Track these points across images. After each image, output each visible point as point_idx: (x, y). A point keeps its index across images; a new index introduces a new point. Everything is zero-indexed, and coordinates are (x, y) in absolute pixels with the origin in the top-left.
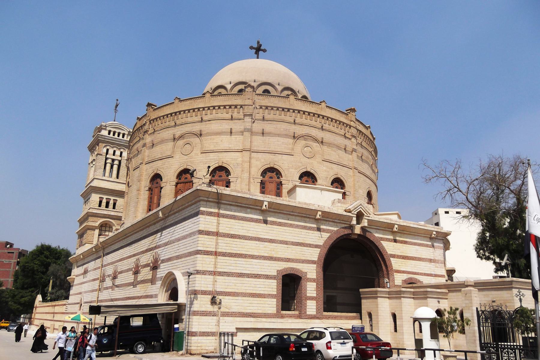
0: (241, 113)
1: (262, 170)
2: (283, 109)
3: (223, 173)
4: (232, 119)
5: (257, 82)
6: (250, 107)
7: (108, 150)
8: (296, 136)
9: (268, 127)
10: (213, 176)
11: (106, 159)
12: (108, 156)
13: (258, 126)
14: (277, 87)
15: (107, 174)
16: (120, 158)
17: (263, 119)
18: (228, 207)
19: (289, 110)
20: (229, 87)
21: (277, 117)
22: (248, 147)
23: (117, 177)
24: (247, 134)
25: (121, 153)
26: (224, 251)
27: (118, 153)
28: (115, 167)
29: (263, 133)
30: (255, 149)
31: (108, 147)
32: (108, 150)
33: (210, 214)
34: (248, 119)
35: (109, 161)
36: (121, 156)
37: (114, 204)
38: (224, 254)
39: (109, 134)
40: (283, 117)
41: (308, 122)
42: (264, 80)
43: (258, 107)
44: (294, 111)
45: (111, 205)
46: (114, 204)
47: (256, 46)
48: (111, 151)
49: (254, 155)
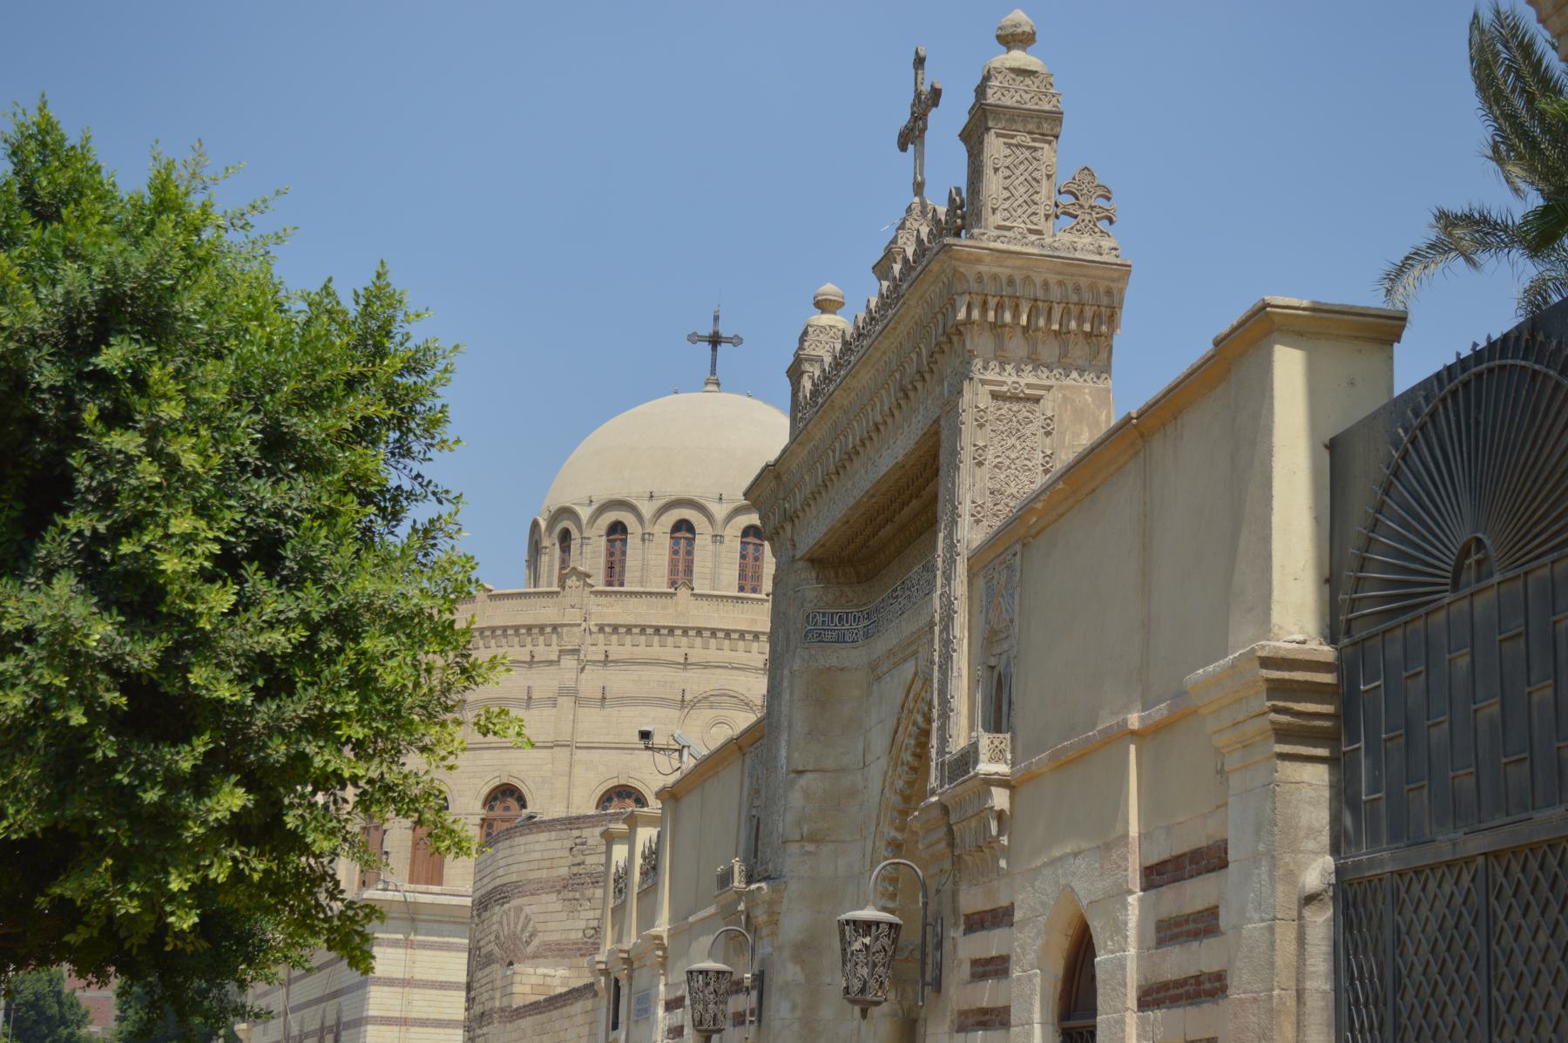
0: (555, 648)
1: (599, 793)
2: (657, 630)
3: (512, 802)
4: (531, 663)
5: (659, 498)
6: (576, 629)
8: (688, 697)
9: (620, 681)
10: (491, 808)
13: (591, 682)
14: (714, 508)
17: (606, 661)
18: (436, 926)
19: (671, 630)
20: (585, 513)
21: (642, 652)
22: (565, 737)
24: (565, 702)
26: (424, 1016)
29: (604, 698)
30: (583, 738)
33: (395, 944)
34: (569, 662)
38: (423, 1023)
40: (656, 651)
41: (726, 655)
42: (677, 490)
43: (595, 629)
44: (685, 631)
47: (707, 331)
49: (580, 754)
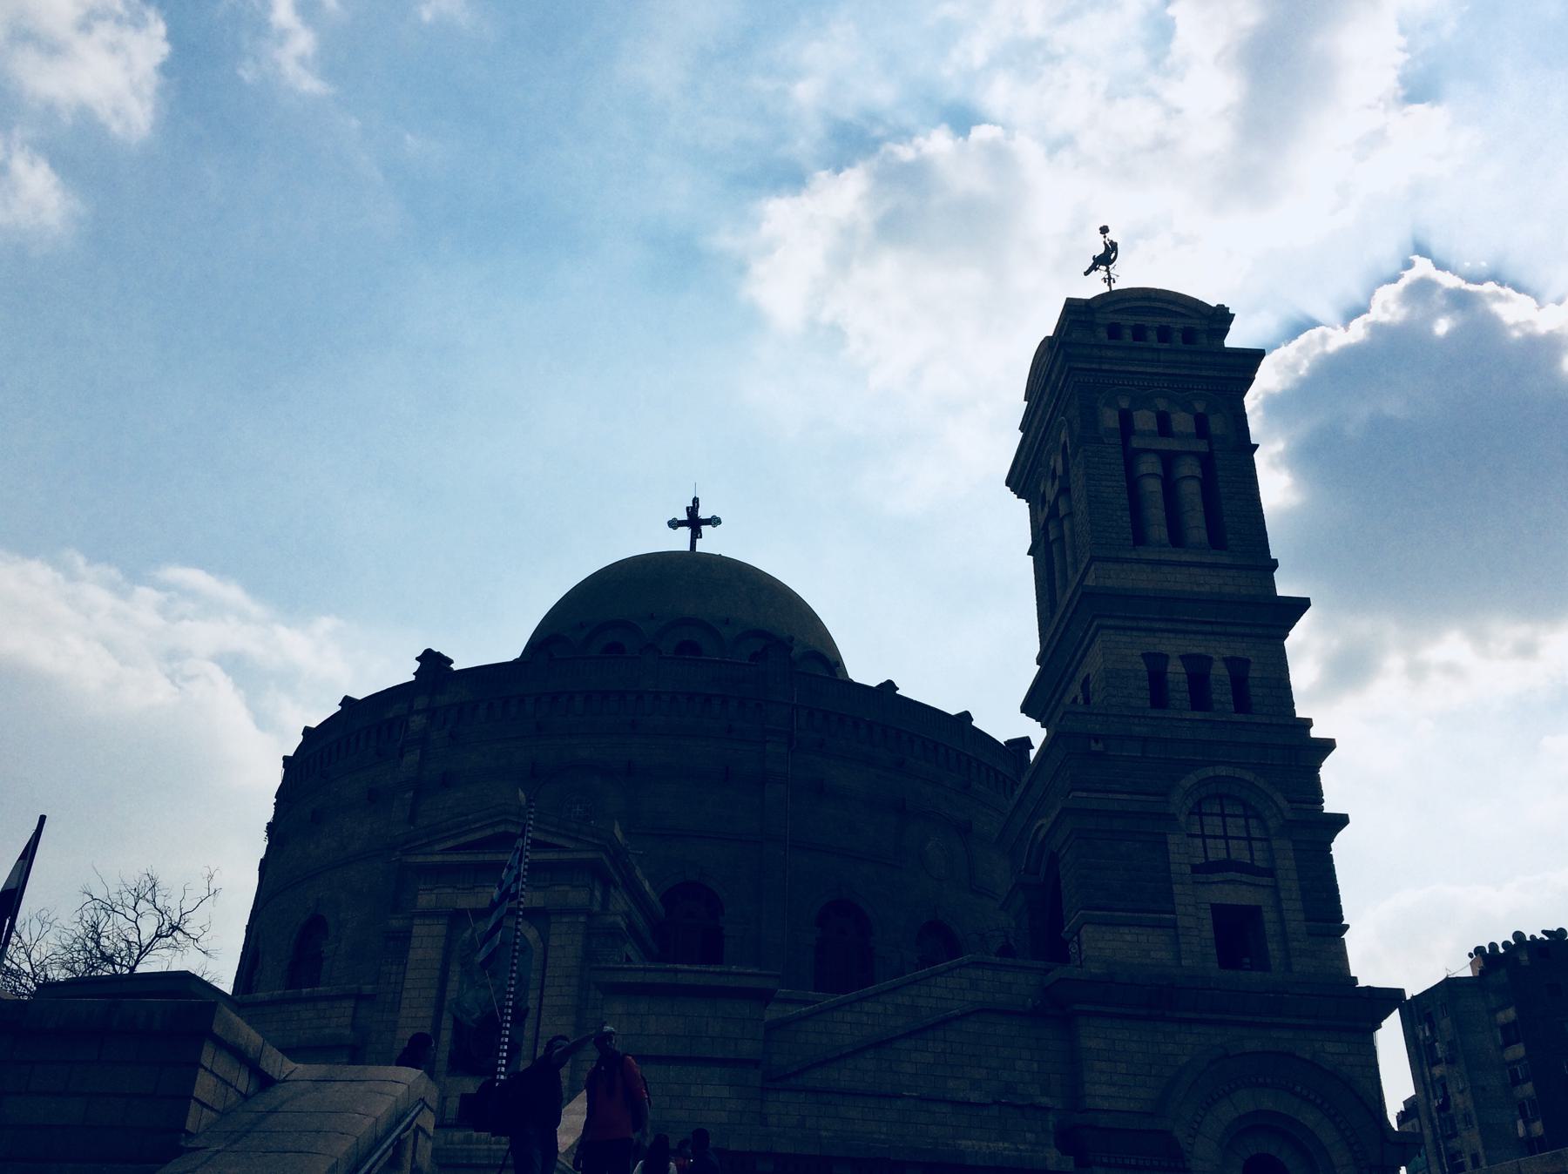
7: (1126, 418)
11: (1130, 458)
12: (1135, 443)
15: (1158, 530)
16: (1202, 446)
23: (1216, 539)
25: (1201, 422)
27: (1182, 422)
28: (1191, 491)
31: (1124, 404)
32: (1126, 418)
35: (1149, 464)
36: (1202, 429)
37: (1239, 685)
39: (1114, 331)
45: (1221, 694)
46: (1239, 685)
48: (1144, 420)
